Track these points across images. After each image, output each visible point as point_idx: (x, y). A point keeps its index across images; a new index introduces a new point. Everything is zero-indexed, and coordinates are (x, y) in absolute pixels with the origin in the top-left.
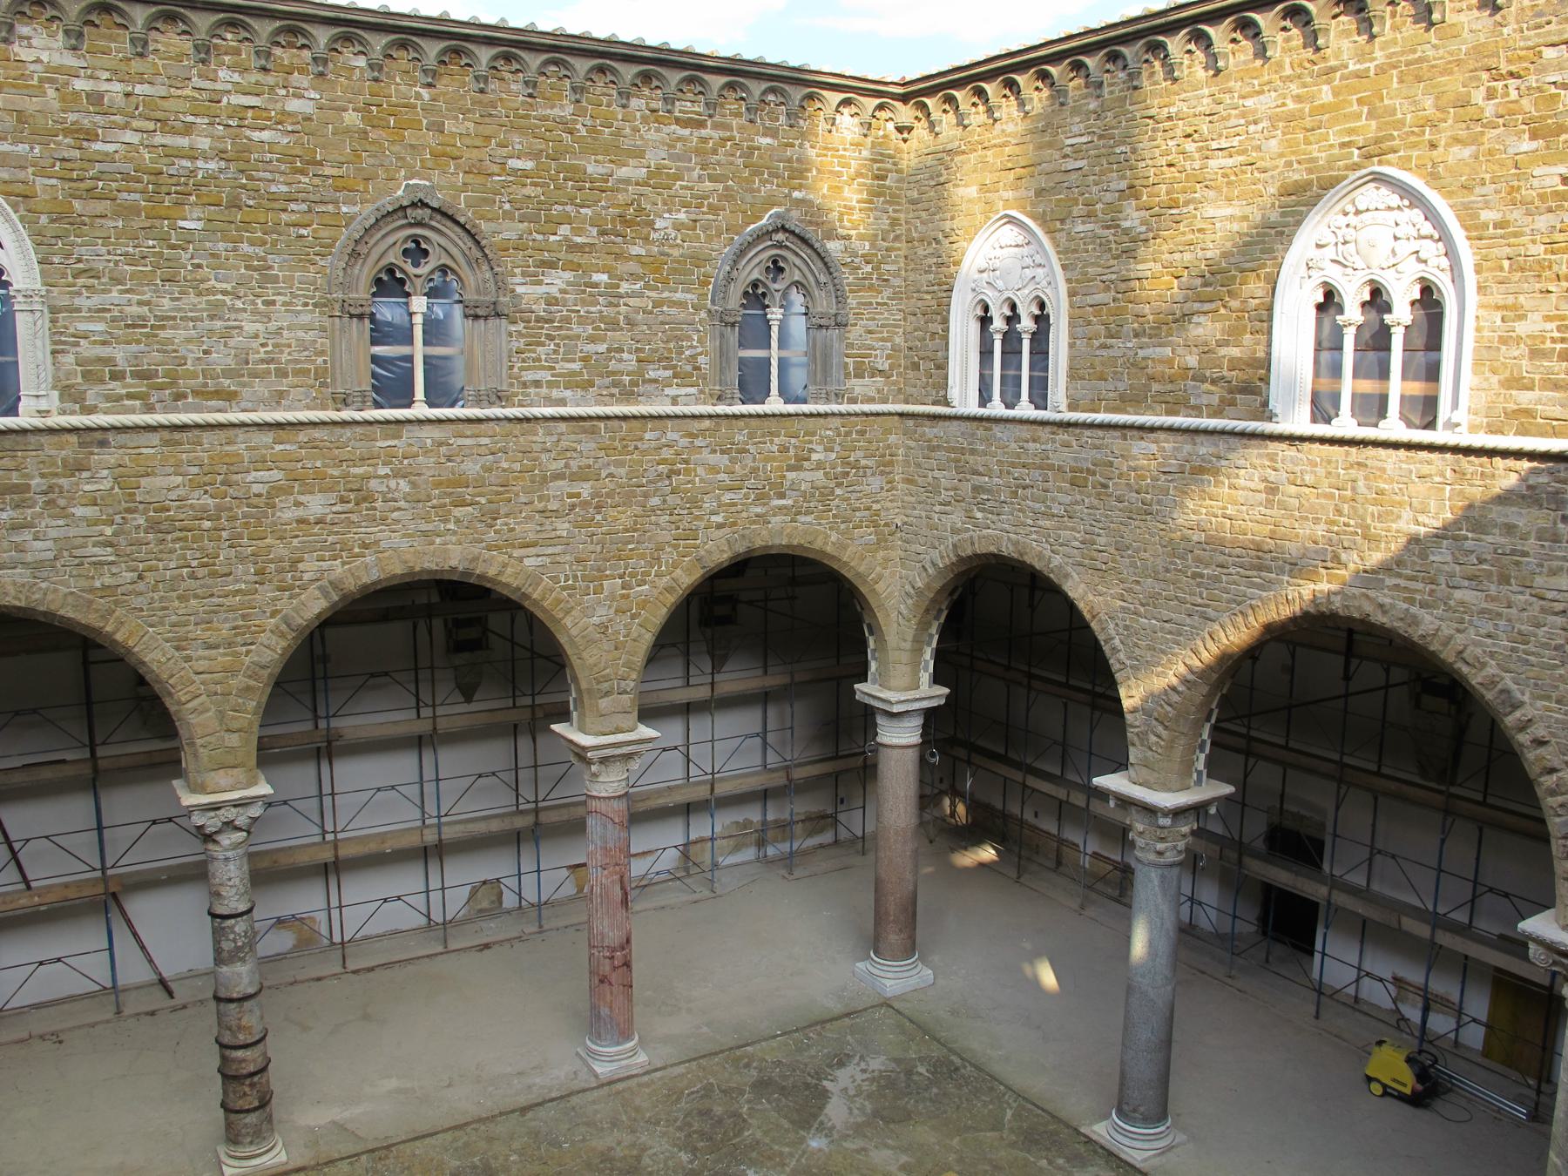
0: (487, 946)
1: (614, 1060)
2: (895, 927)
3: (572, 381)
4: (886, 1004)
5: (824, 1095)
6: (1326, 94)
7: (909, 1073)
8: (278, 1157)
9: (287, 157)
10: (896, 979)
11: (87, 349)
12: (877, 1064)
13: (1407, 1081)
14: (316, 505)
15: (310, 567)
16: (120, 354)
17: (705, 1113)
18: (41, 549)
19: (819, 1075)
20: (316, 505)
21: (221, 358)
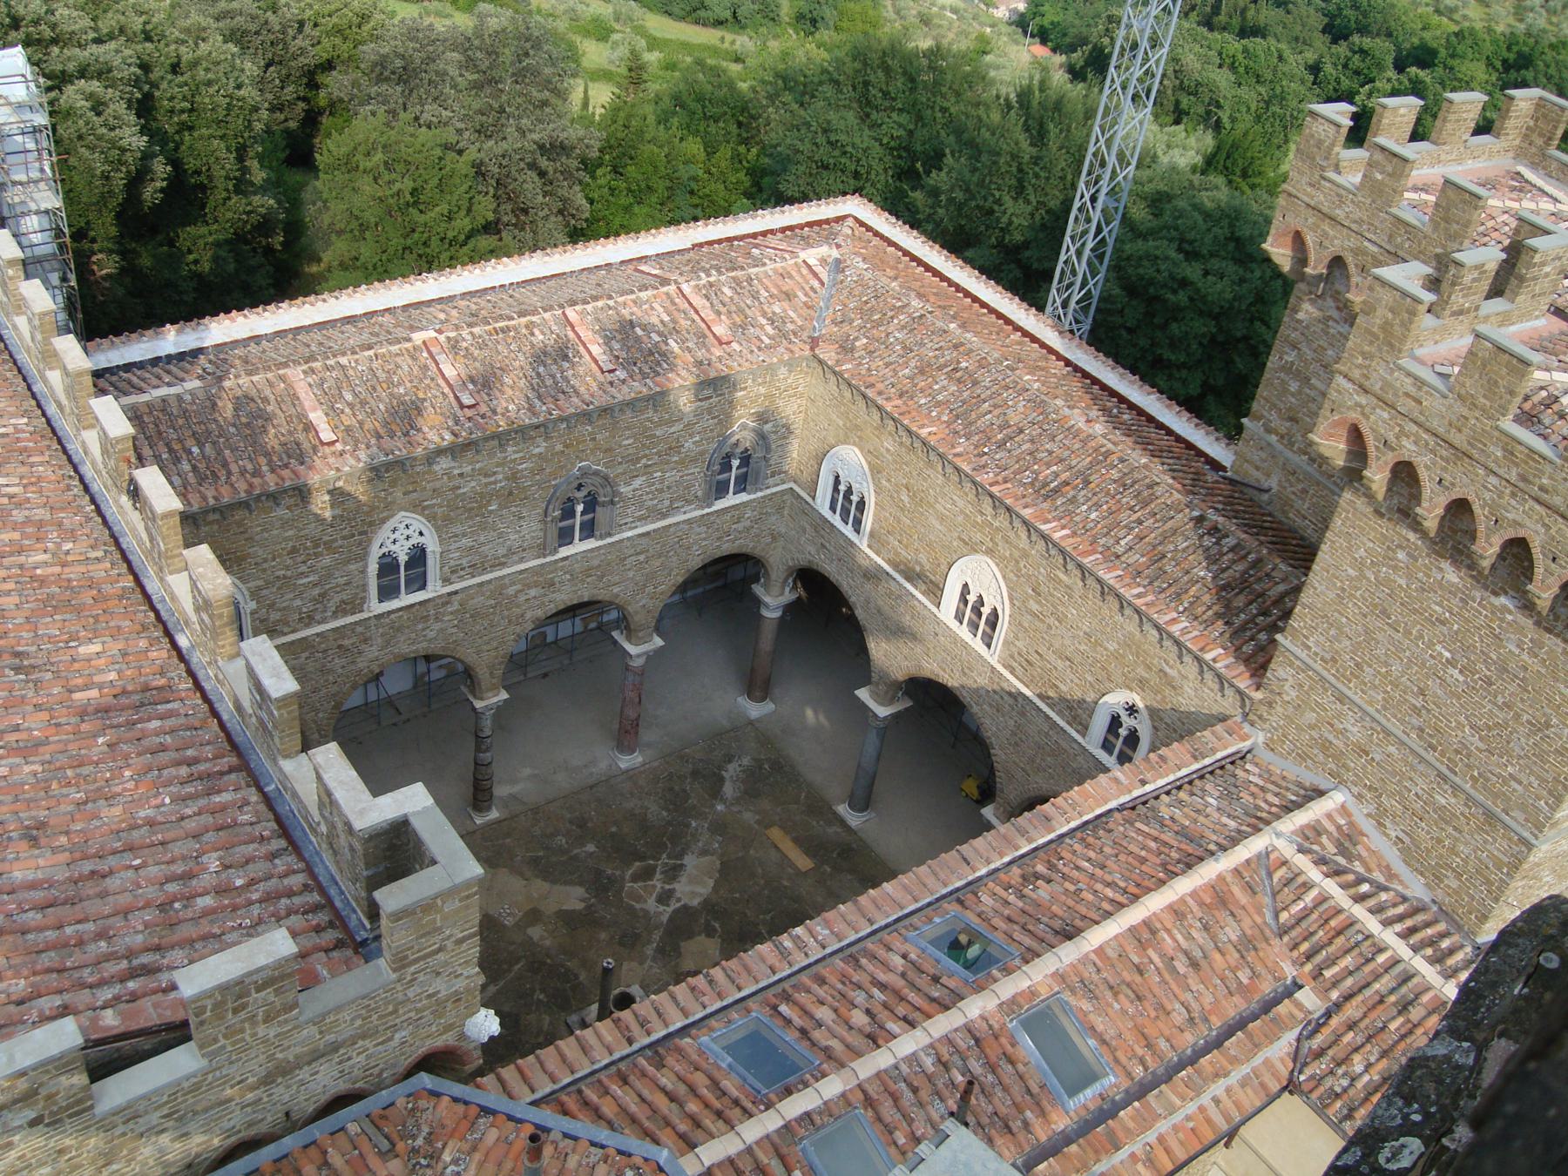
0: (545, 675)
1: (626, 762)
2: (758, 686)
3: (640, 519)
4: (751, 723)
5: (722, 780)
6: (979, 519)
7: (761, 768)
8: (494, 814)
9: (532, 471)
10: (755, 710)
11: (452, 563)
12: (746, 761)
13: (975, 794)
14: (533, 592)
15: (528, 615)
16: (464, 562)
17: (671, 789)
18: (432, 634)
19: (720, 768)
20: (533, 592)
21: (502, 551)
